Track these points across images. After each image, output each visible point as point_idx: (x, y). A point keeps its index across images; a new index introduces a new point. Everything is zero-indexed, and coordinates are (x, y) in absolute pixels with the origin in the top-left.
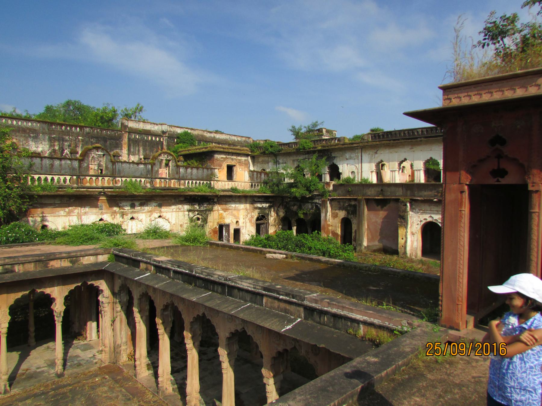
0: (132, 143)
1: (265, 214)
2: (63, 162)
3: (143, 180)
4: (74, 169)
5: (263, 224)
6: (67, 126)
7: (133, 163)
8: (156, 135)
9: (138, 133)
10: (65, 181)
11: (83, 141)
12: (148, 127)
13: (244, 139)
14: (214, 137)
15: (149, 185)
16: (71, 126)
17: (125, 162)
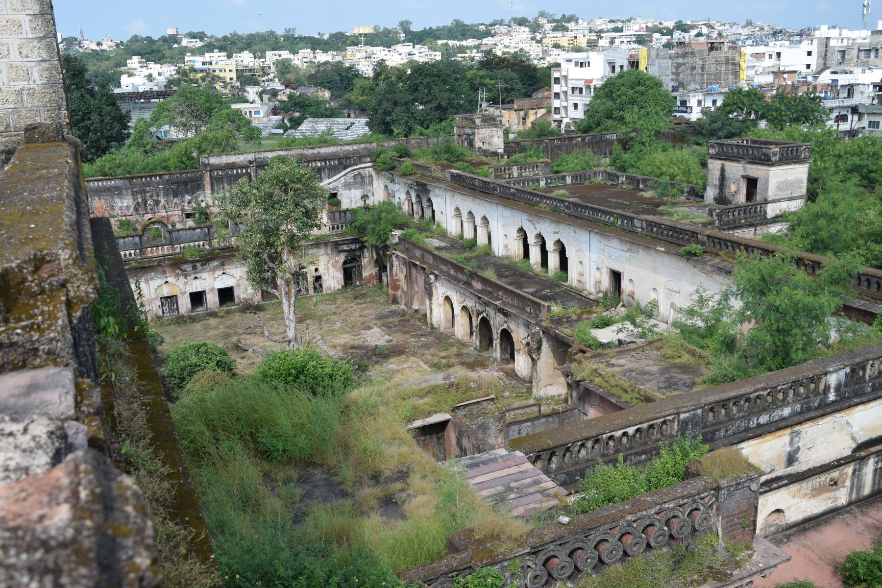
0: (216, 181)
1: (357, 256)
2: (126, 239)
3: (201, 243)
4: (136, 244)
5: (354, 267)
6: (146, 177)
7: (190, 229)
8: (242, 168)
9: (221, 170)
10: (130, 255)
11: (163, 189)
12: (232, 159)
13: (363, 146)
14: (319, 153)
15: (207, 247)
16: (151, 177)
17: (182, 229)
